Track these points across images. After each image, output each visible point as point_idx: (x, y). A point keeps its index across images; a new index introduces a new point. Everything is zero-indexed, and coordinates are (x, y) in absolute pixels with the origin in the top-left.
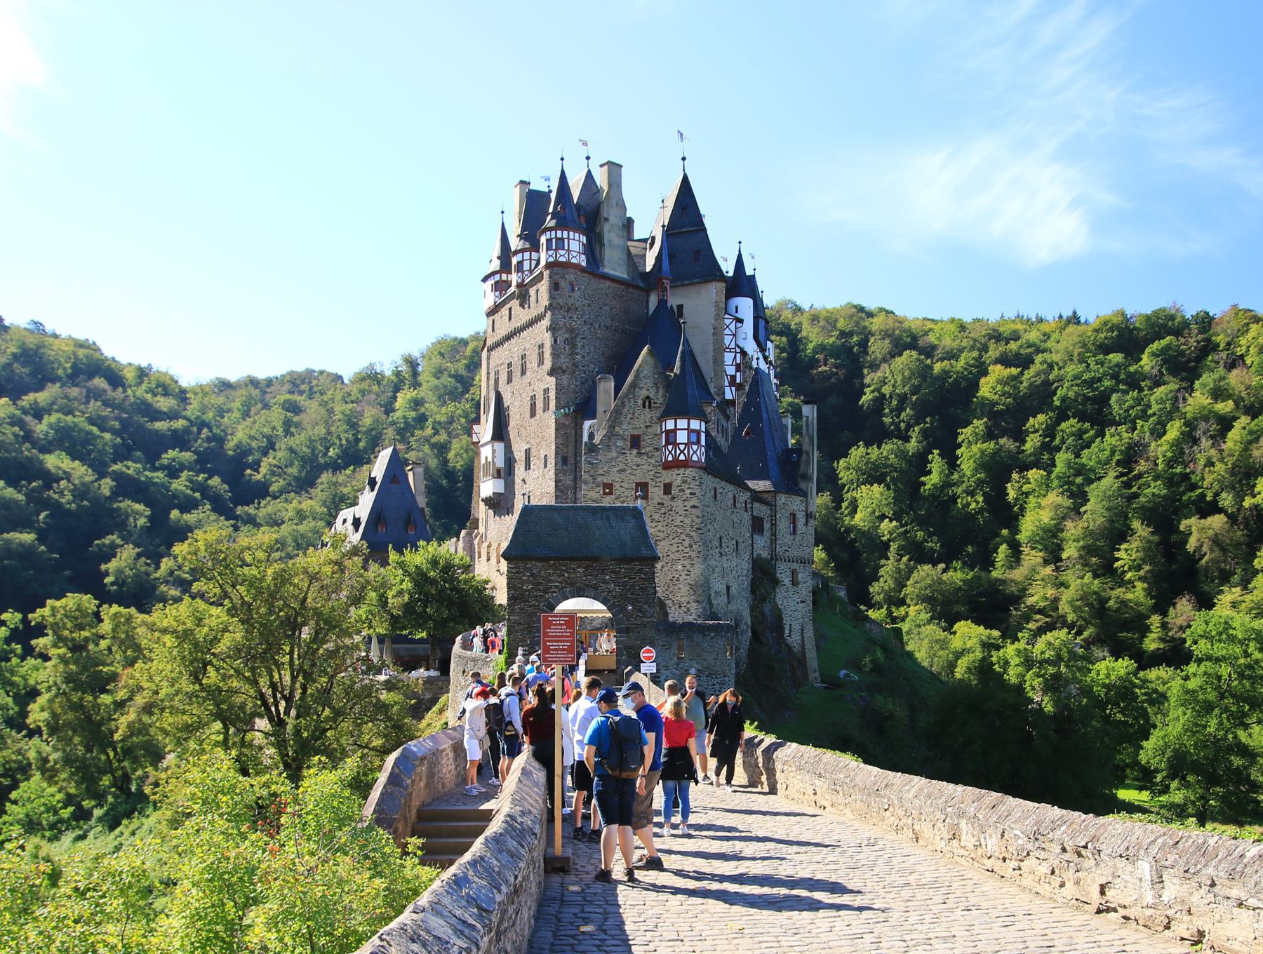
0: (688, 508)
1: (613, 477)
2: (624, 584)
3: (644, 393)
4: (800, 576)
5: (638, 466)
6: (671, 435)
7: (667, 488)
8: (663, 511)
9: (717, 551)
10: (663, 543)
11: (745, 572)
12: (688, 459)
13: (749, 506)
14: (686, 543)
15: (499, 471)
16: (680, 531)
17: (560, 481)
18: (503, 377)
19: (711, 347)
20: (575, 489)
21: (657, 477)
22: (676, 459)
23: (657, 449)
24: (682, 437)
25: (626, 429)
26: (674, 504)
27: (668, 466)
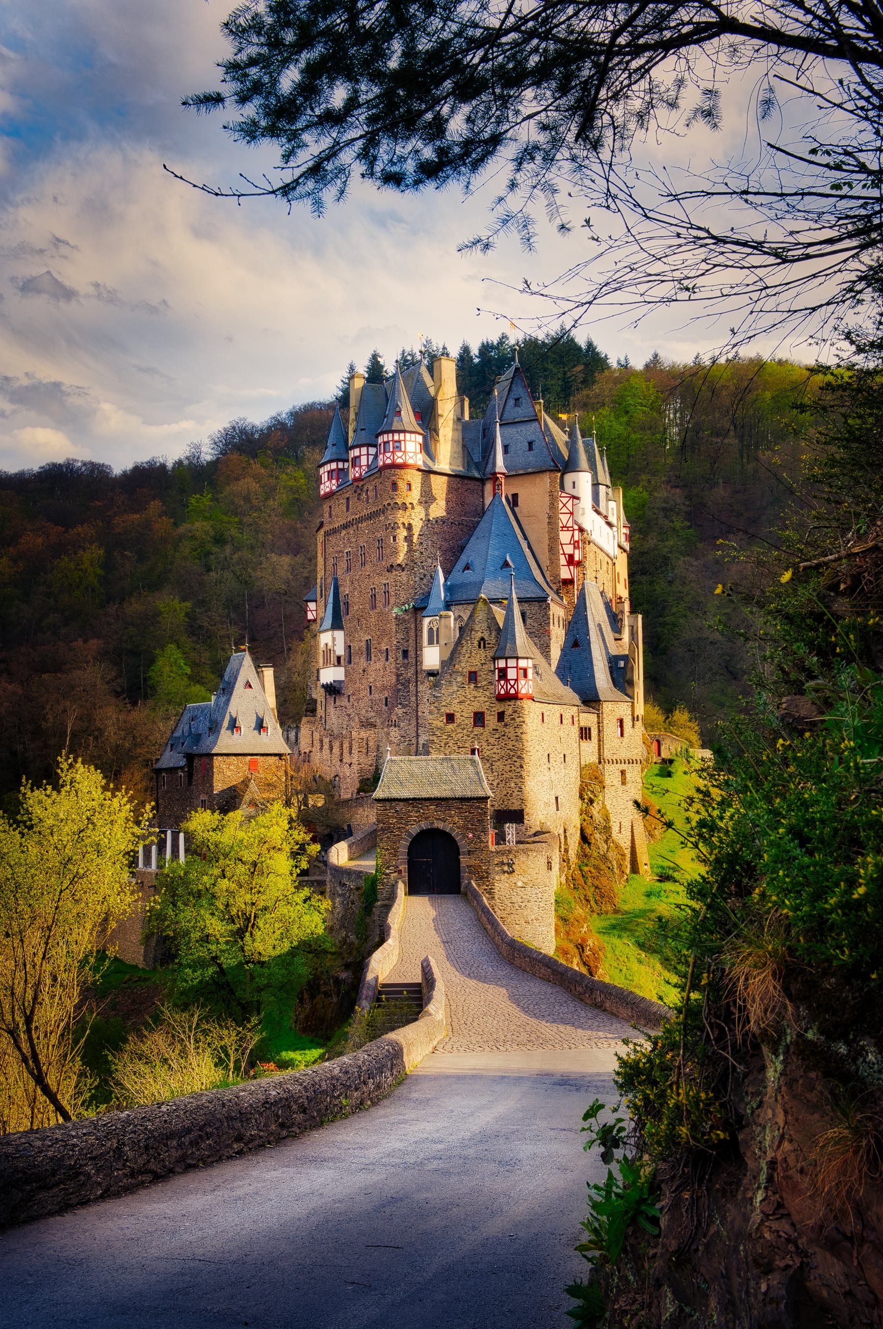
0: (519, 734)
1: (454, 708)
2: (466, 818)
3: (479, 635)
4: (628, 776)
5: (475, 697)
6: (503, 673)
7: (501, 716)
8: (497, 736)
9: (545, 767)
10: (498, 763)
11: (574, 779)
12: (517, 693)
13: (576, 719)
14: (517, 764)
15: (339, 658)
16: (512, 753)
17: (402, 674)
18: (343, 565)
19: (547, 535)
20: (417, 682)
21: (492, 707)
22: (507, 692)
23: (491, 683)
24: (511, 674)
25: (464, 665)
26: (507, 730)
27: (501, 699)
